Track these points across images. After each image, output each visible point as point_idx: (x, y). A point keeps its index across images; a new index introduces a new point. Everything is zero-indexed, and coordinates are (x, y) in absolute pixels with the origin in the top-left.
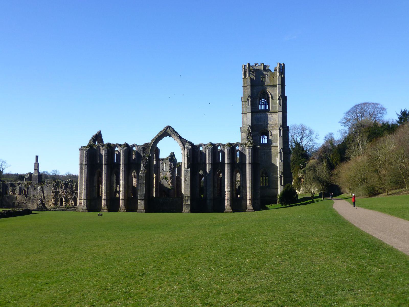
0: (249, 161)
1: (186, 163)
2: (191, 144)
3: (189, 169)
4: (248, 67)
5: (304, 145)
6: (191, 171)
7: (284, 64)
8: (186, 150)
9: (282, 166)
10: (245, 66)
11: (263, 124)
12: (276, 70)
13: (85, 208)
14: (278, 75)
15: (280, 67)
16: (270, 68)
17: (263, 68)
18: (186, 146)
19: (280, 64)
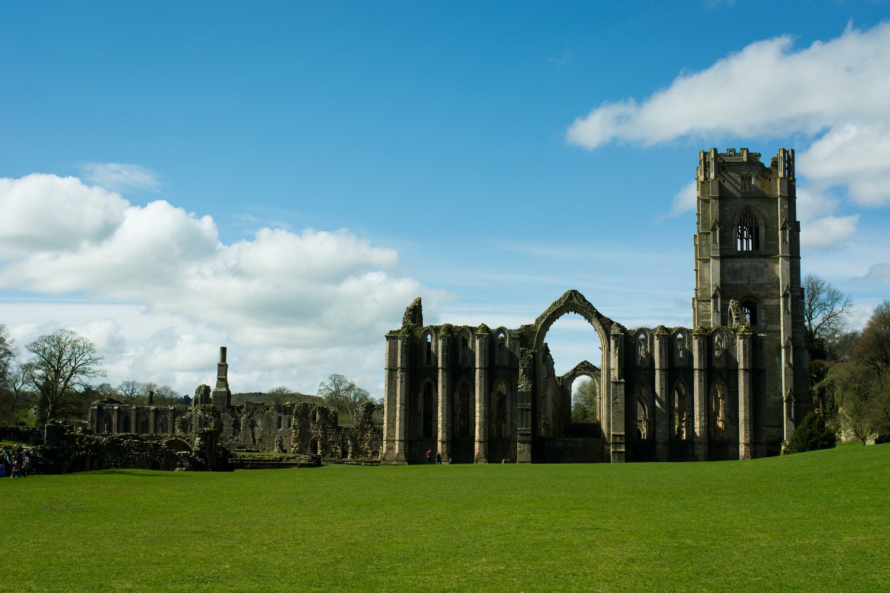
0: (744, 366)
1: (612, 366)
2: (623, 329)
3: (623, 380)
4: (713, 156)
5: (813, 328)
6: (626, 384)
7: (793, 151)
8: (612, 342)
9: (791, 378)
10: (705, 154)
11: (746, 282)
12: (775, 163)
13: (402, 457)
14: (781, 174)
15: (784, 157)
16: (761, 160)
17: (745, 160)
18: (612, 332)
19: (785, 151)
